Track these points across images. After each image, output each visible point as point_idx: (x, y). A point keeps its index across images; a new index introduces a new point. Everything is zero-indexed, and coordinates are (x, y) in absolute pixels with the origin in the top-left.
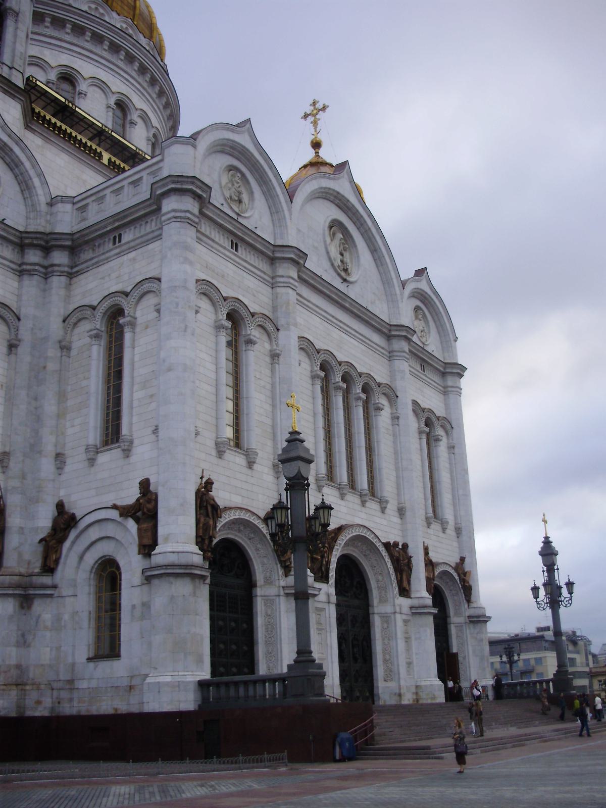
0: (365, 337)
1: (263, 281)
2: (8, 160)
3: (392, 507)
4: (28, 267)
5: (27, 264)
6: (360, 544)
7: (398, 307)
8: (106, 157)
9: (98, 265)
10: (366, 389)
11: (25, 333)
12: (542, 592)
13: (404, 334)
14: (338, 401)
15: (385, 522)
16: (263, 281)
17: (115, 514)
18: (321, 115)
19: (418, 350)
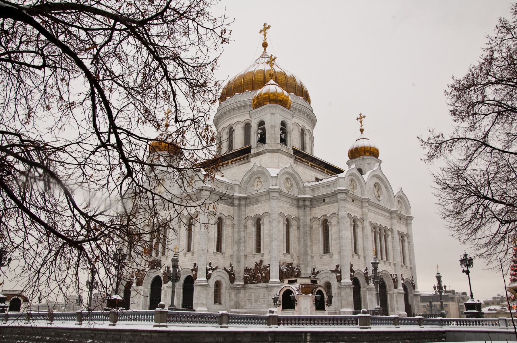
1: (360, 208)
3: (392, 264)
8: (310, 163)
9: (319, 206)
11: (301, 224)
12: (436, 288)
14: (378, 236)
17: (330, 272)
18: (363, 119)
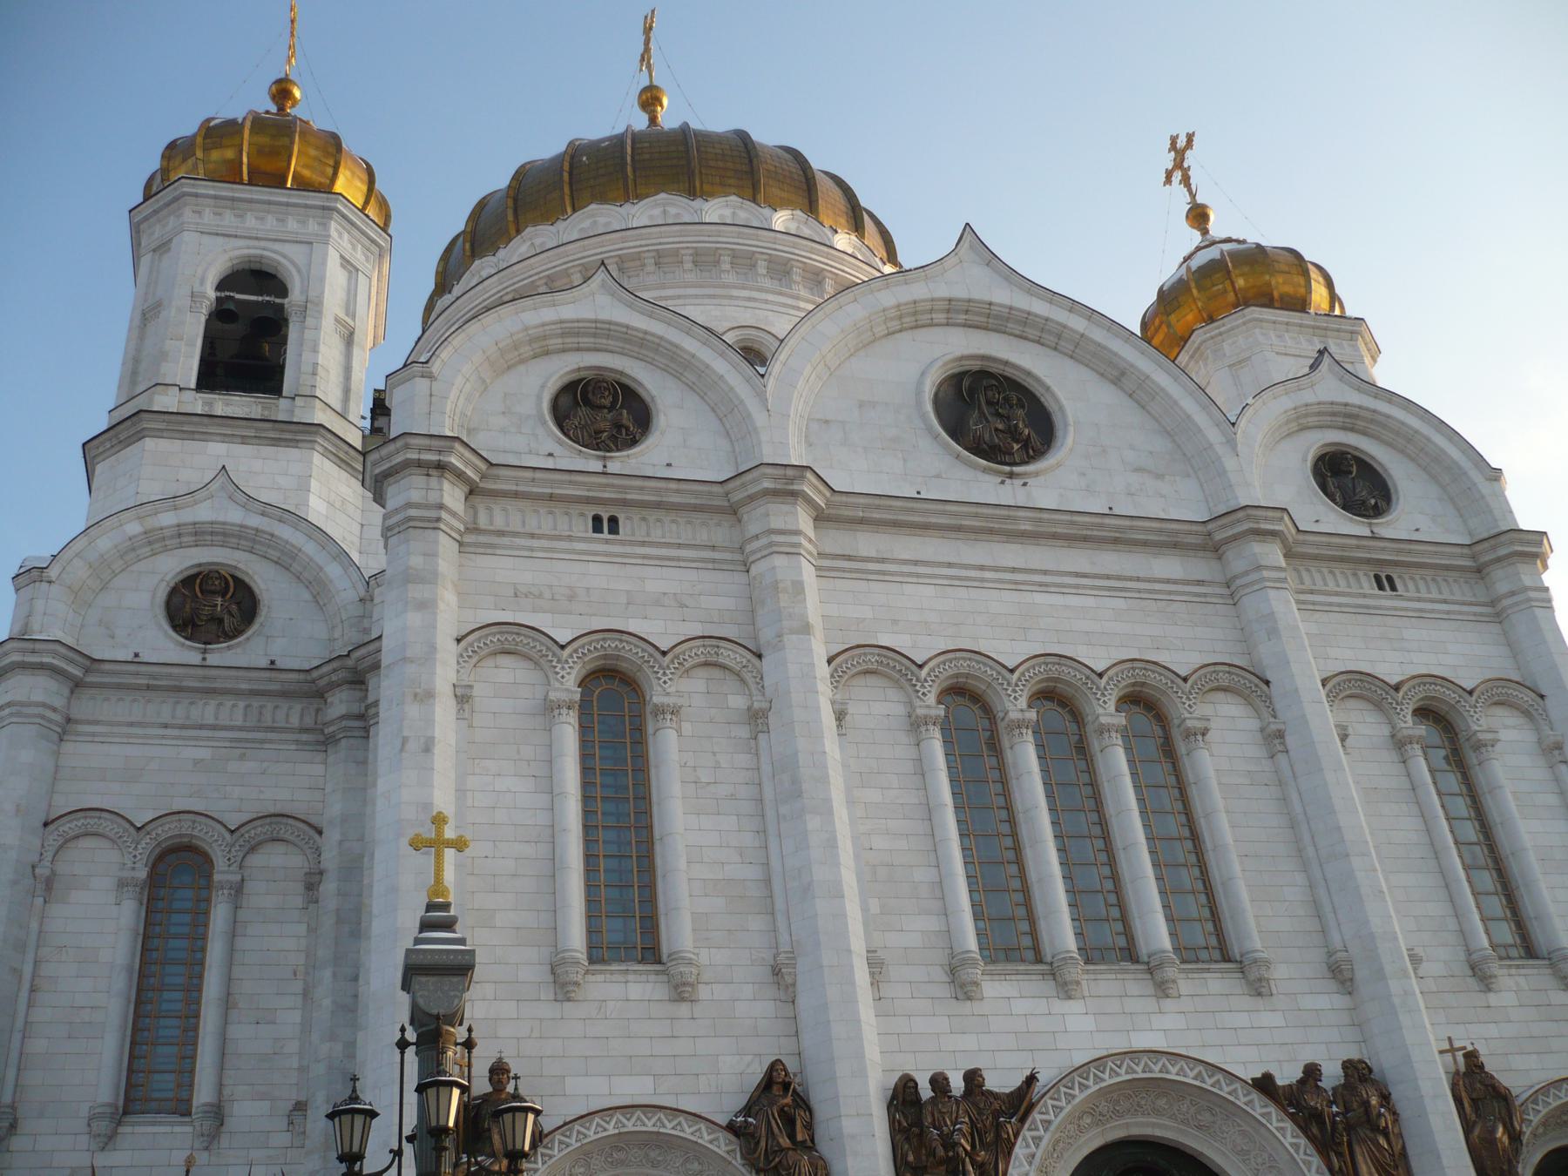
0: (1119, 578)
1: (716, 565)
2: (274, 554)
4: (331, 729)
5: (332, 722)
6: (1162, 1102)
7: (1222, 473)
10: (1142, 701)
13: (1245, 526)
15: (1275, 1019)
16: (710, 566)
19: (1343, 547)
